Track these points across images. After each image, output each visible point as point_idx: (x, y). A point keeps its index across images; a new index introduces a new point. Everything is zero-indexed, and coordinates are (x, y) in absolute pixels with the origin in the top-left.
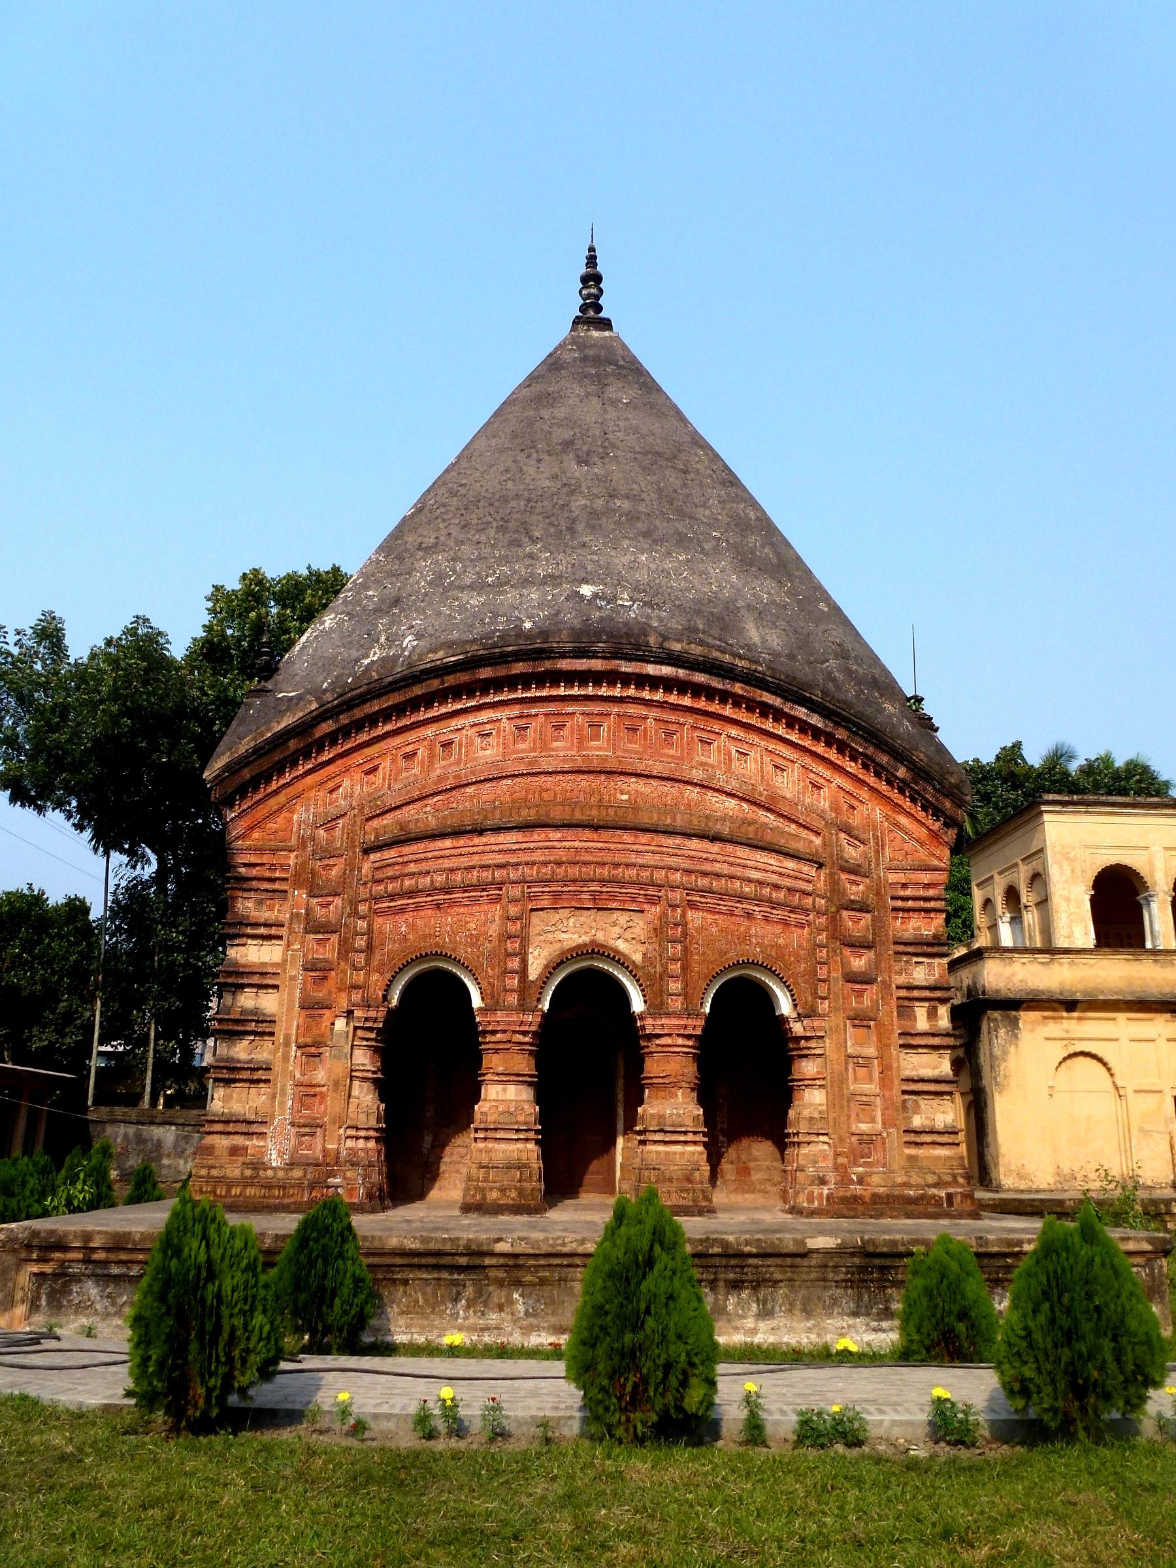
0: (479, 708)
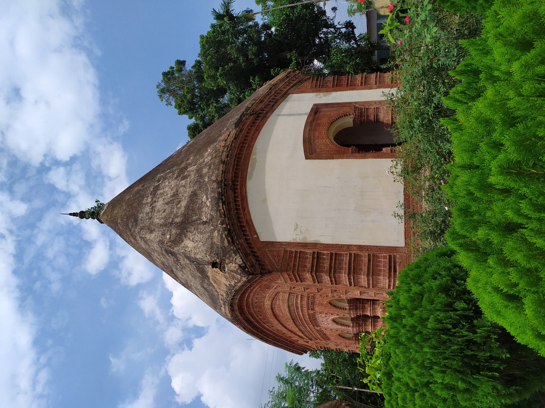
0: (265, 328)
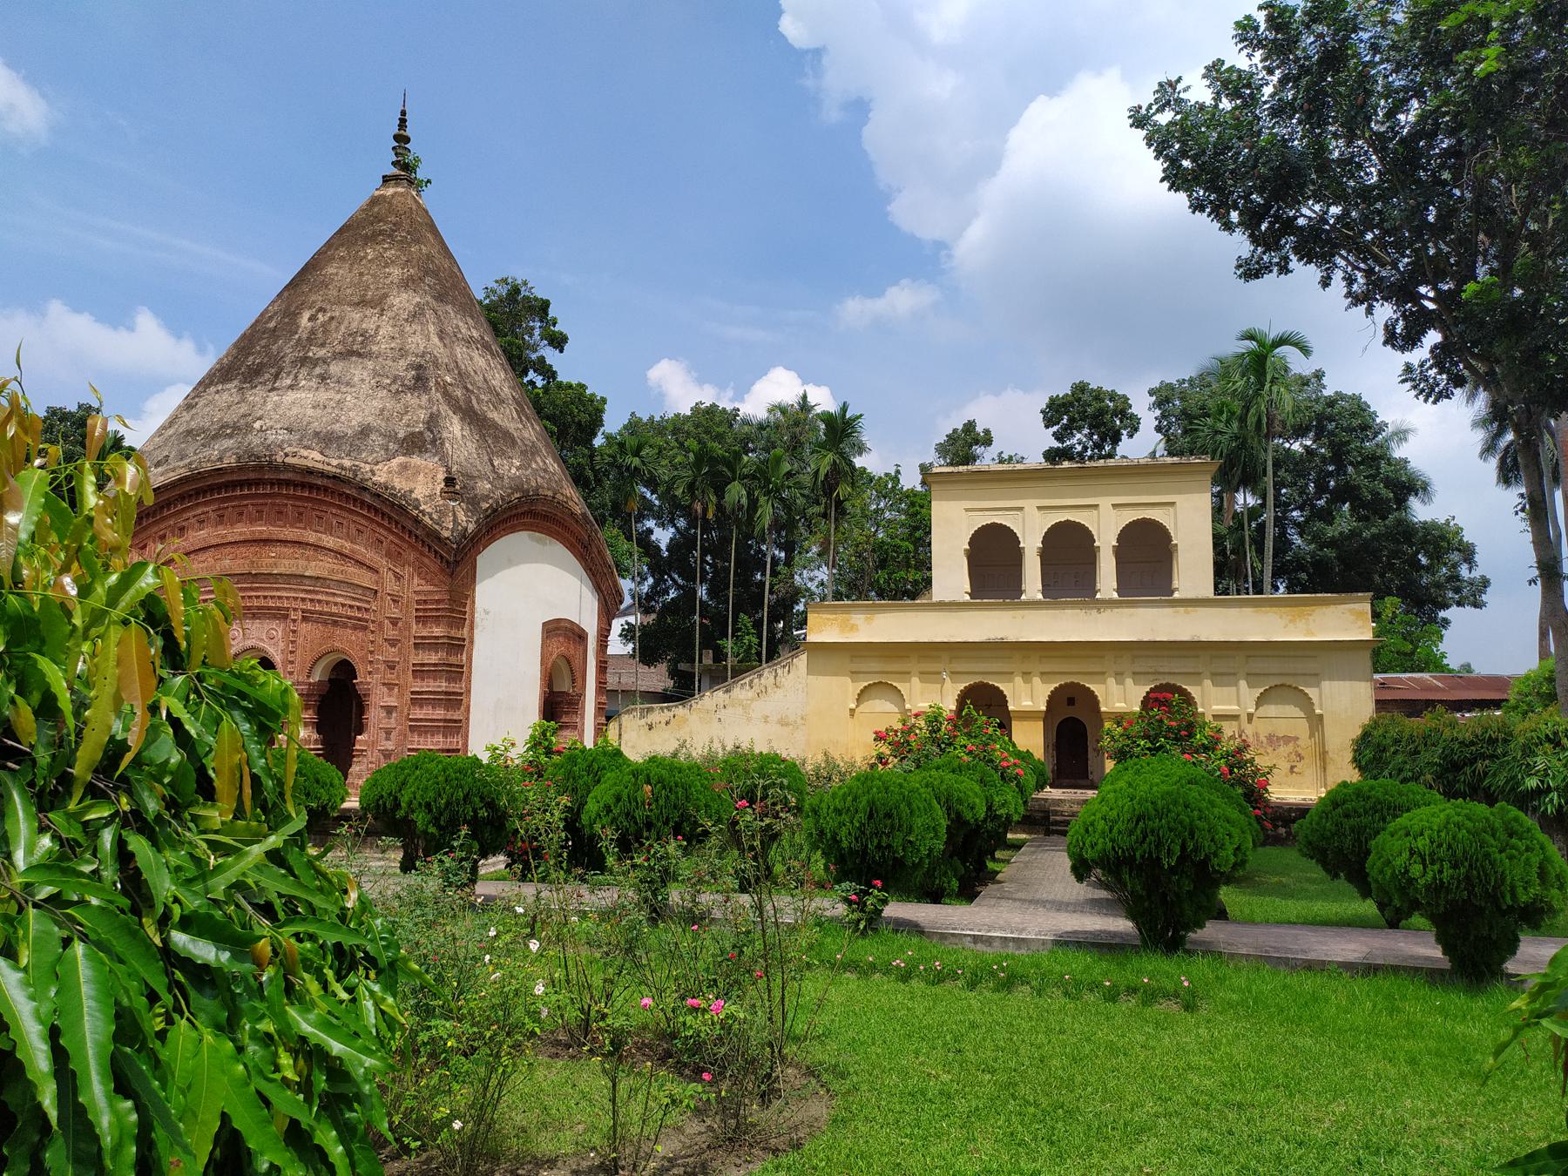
0: (198, 504)
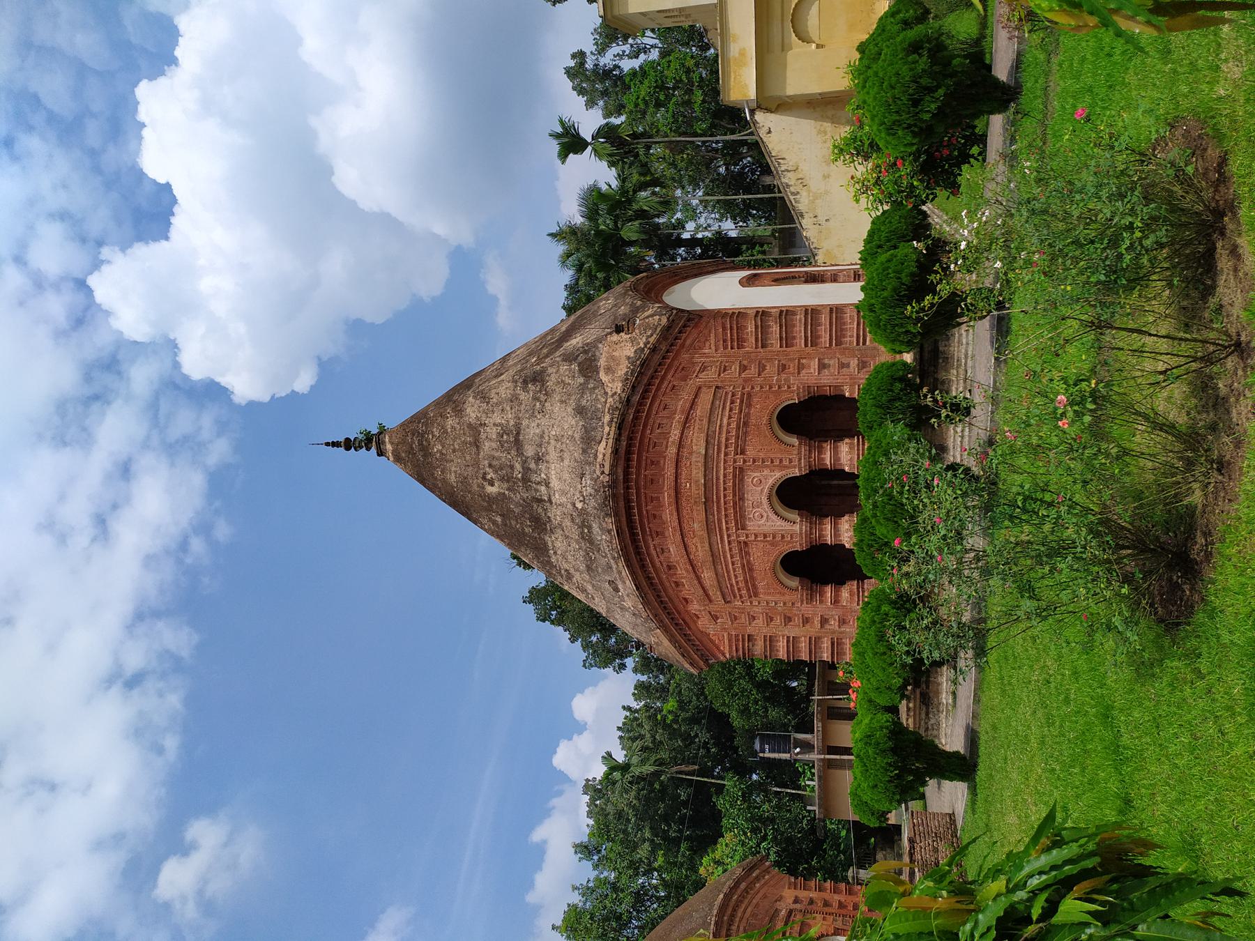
0: (649, 555)
